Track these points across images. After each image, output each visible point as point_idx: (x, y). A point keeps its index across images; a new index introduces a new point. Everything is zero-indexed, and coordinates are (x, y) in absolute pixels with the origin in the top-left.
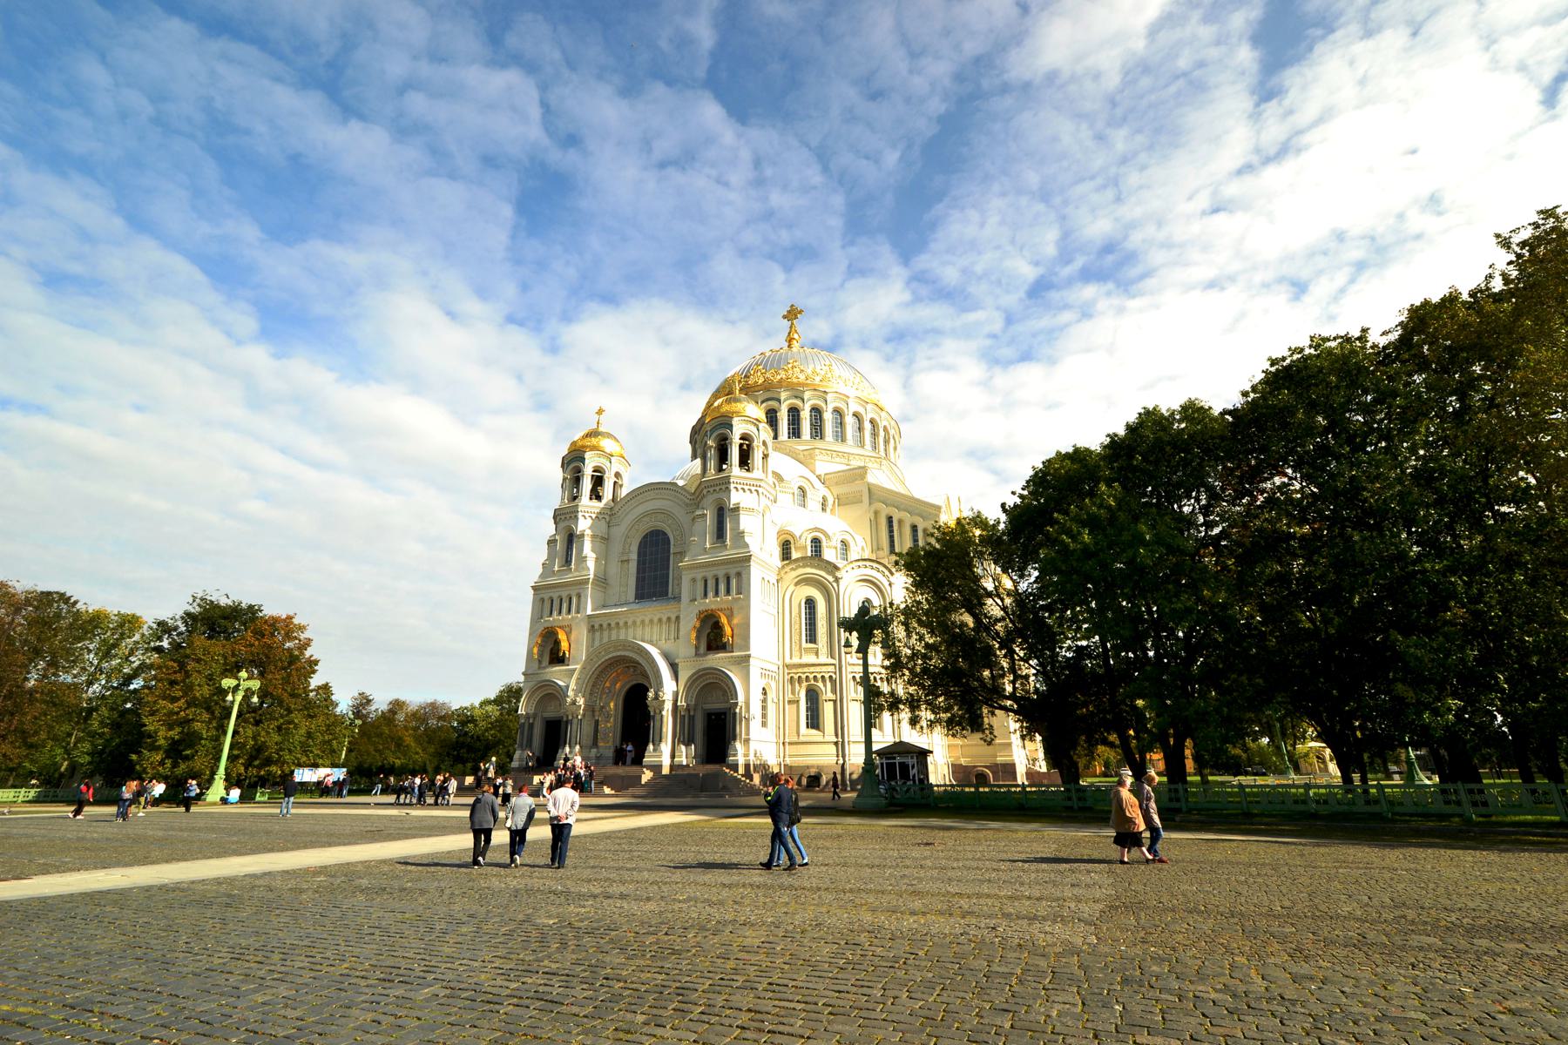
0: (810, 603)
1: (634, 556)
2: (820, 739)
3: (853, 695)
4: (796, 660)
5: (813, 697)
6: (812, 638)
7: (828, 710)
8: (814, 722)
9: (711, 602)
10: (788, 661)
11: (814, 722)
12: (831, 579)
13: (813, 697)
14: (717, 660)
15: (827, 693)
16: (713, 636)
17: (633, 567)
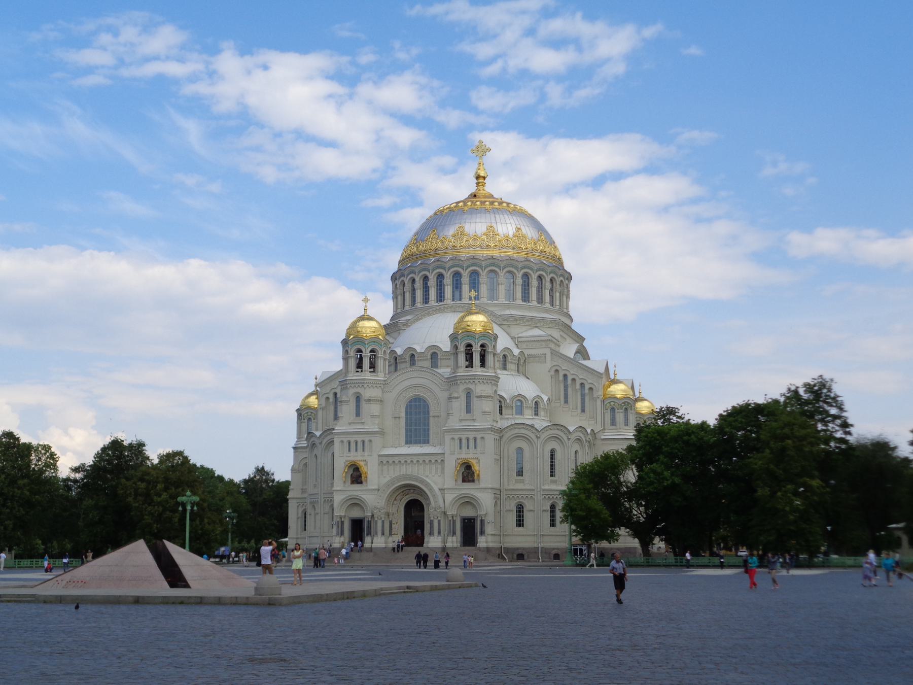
0: (520, 450)
1: (403, 415)
2: (525, 533)
3: (544, 508)
4: (512, 487)
5: (520, 510)
6: (520, 473)
7: (528, 517)
8: (520, 522)
9: (468, 455)
10: (506, 487)
11: (520, 522)
12: (533, 437)
13: (520, 510)
14: (468, 489)
15: (528, 506)
16: (468, 473)
17: (403, 422)
